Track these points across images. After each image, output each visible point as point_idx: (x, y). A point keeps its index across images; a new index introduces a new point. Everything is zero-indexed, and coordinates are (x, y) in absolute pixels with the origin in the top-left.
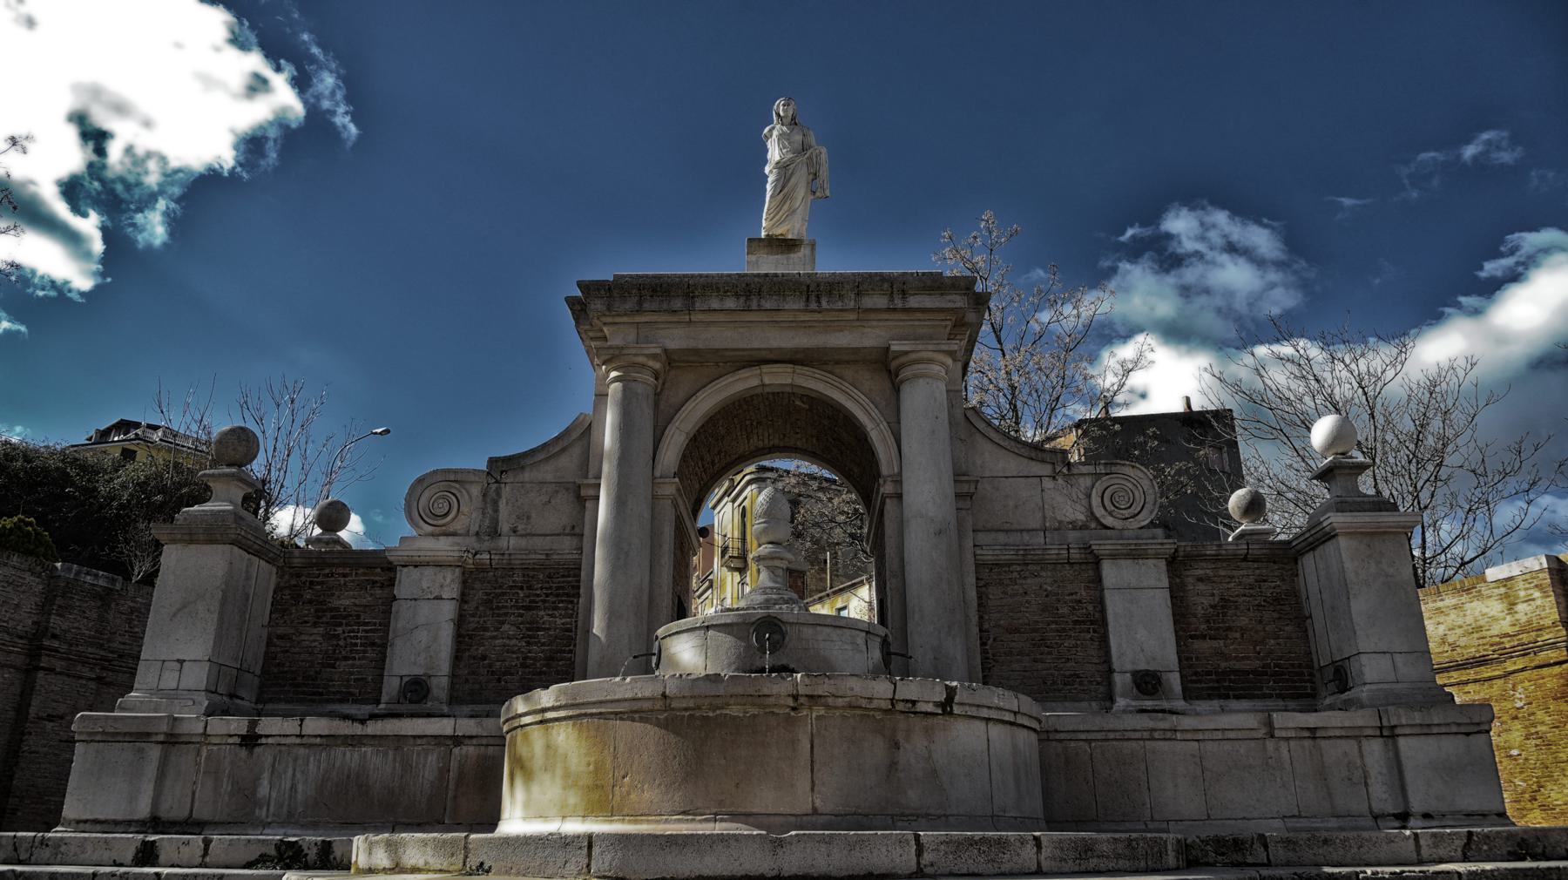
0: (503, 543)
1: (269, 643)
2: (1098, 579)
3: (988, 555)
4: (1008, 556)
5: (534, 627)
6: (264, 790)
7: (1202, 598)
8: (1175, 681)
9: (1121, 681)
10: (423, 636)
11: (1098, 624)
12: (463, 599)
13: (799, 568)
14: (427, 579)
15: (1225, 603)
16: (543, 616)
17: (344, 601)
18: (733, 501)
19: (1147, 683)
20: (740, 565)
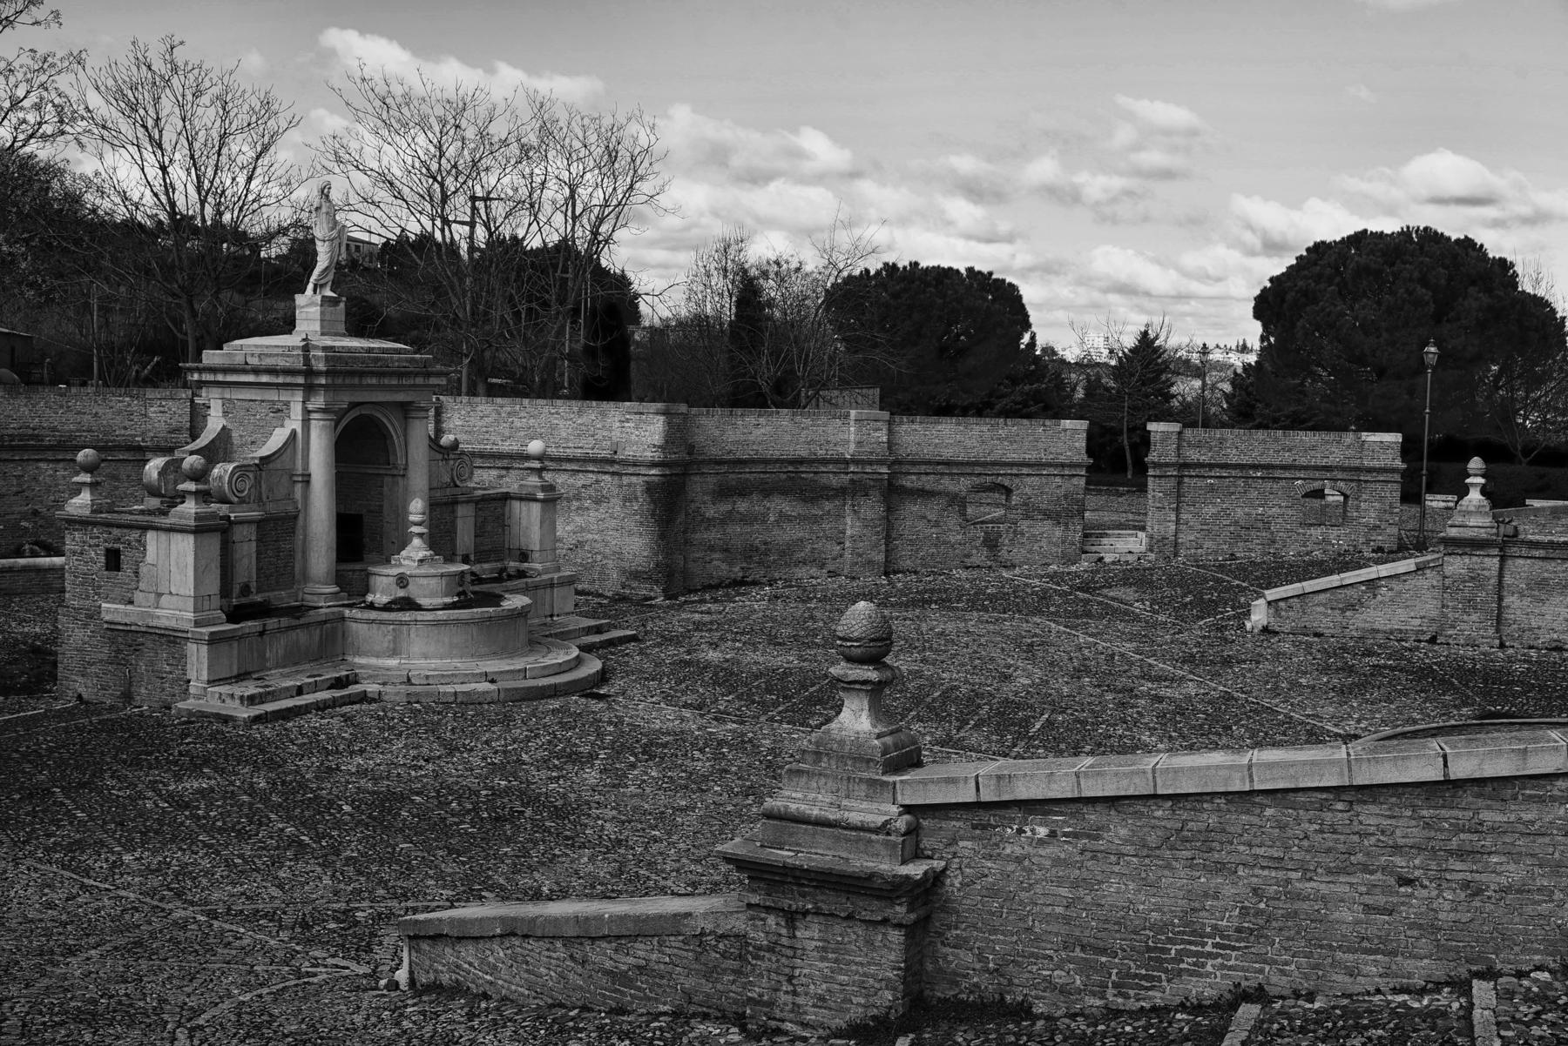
10: (246, 561)
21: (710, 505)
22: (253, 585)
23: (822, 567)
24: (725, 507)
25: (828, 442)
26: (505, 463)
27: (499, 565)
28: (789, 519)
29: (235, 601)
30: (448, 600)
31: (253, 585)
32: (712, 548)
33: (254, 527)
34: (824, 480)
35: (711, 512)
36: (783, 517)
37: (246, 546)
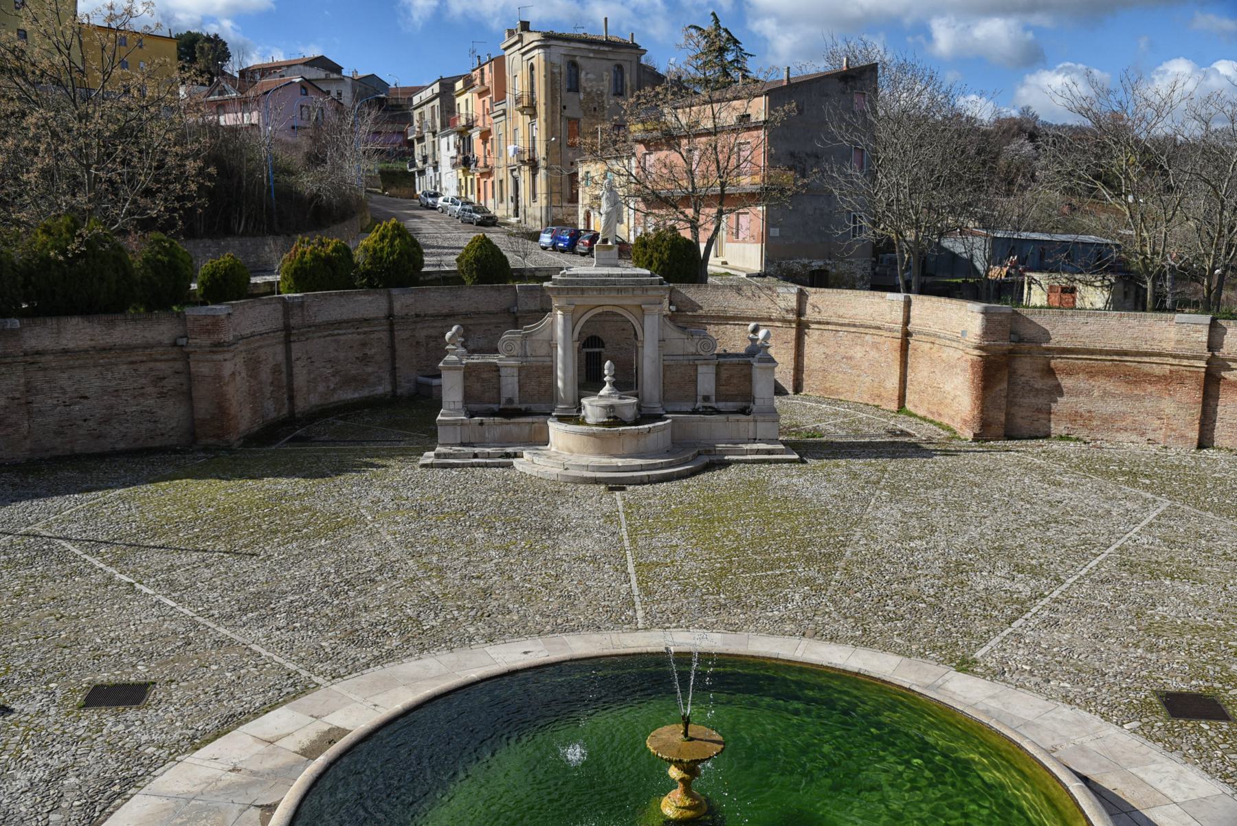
0: (529, 359)
2: (697, 370)
3: (666, 363)
4: (672, 363)
5: (540, 383)
6: (487, 435)
7: (724, 374)
9: (699, 398)
11: (695, 382)
12: (519, 375)
13: (575, 116)
14: (509, 371)
15: (731, 376)
18: (523, 54)
19: (706, 398)
22: (516, 399)
23: (1143, 434)
25: (1153, 339)
26: (932, 339)
27: (744, 404)
29: (501, 406)
30: (601, 420)
31: (516, 399)
34: (1146, 368)
36: (1105, 394)
37: (510, 379)
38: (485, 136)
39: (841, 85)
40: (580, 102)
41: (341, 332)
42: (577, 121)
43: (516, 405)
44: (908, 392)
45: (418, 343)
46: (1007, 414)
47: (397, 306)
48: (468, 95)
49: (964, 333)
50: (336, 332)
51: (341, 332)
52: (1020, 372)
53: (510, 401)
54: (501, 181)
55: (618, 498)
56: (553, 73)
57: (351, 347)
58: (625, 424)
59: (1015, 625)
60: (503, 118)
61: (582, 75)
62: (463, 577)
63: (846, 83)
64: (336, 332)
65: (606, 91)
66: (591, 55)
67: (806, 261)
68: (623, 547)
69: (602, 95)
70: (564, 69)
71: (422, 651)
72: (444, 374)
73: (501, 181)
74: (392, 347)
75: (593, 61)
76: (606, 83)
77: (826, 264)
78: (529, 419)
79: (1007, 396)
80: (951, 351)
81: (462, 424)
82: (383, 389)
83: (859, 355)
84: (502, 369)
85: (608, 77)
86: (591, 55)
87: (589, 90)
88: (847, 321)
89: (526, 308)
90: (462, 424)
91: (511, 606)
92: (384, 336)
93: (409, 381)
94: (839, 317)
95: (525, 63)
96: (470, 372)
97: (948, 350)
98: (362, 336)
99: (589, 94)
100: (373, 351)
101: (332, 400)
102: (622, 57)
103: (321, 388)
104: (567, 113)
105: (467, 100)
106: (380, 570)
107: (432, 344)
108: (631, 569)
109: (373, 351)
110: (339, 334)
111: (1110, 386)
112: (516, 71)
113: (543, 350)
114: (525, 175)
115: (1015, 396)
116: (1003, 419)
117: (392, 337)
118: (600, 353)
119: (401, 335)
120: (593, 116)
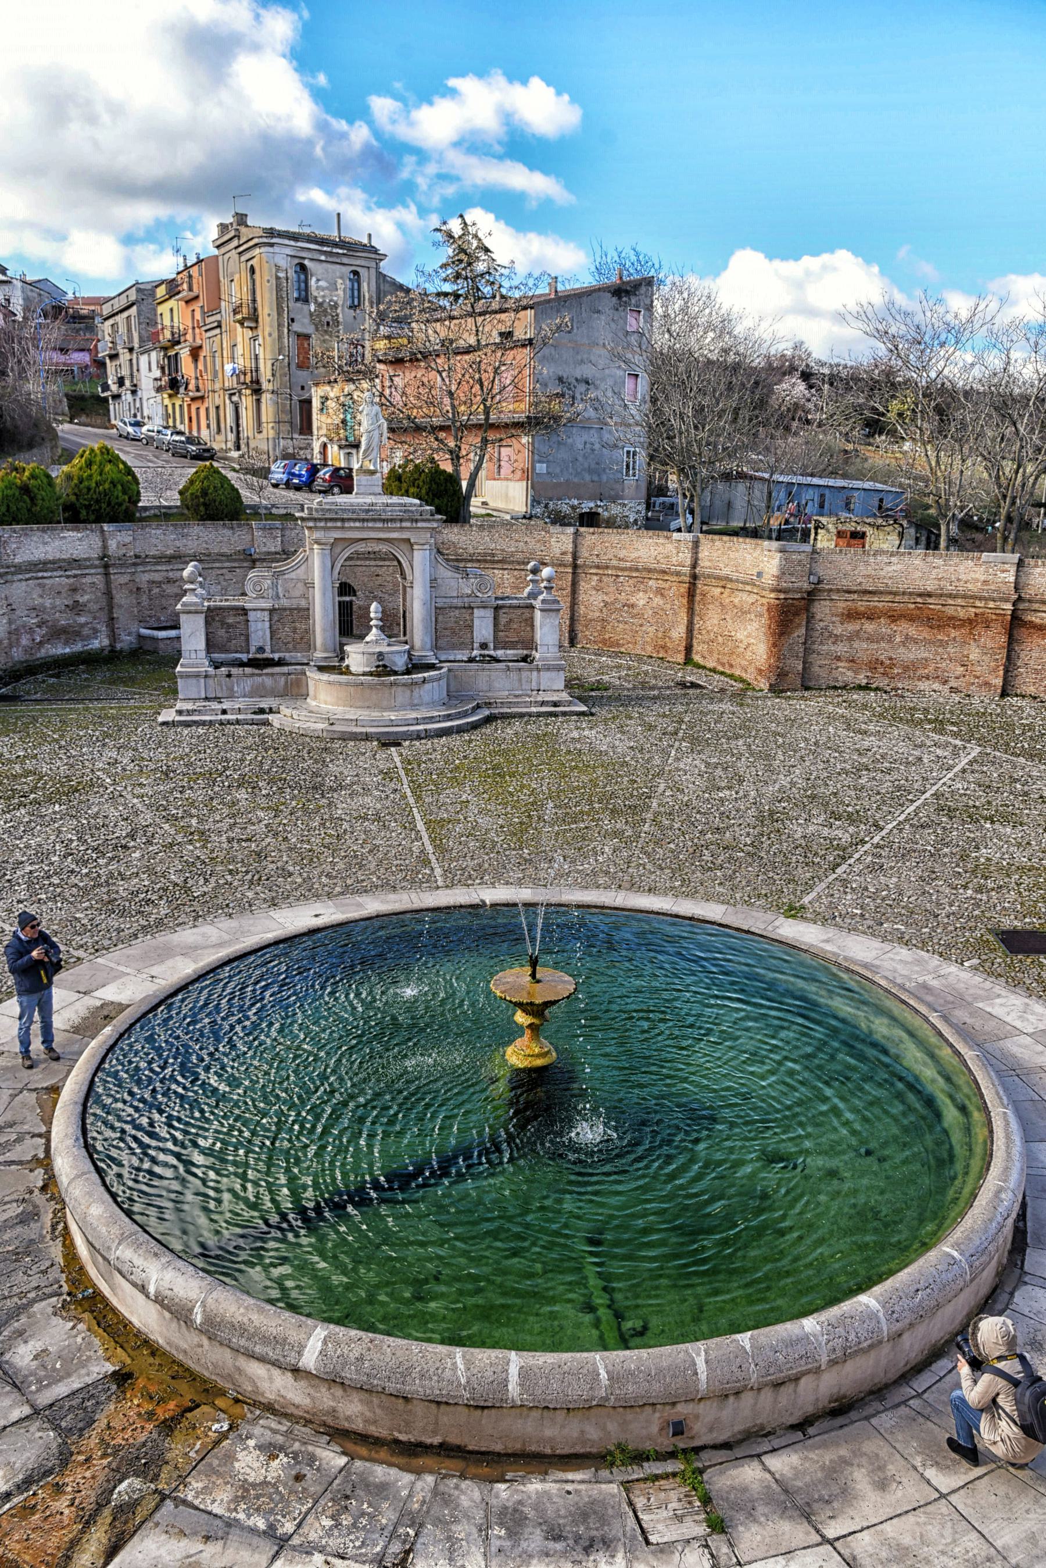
1: (207, 635)
8: (491, 645)
9: (476, 645)
10: (260, 633)
11: (471, 627)
16: (298, 625)
17: (230, 621)
19: (484, 646)
20: (253, 325)
21: (838, 625)
22: (268, 648)
23: (945, 682)
24: (852, 627)
25: (959, 580)
26: (722, 583)
27: (525, 652)
28: (916, 641)
30: (368, 669)
31: (268, 648)
32: (838, 659)
33: (267, 613)
34: (950, 611)
35: (838, 630)
37: (260, 625)
38: (195, 353)
39: (615, 299)
40: (311, 314)
41: (45, 574)
42: (307, 337)
43: (268, 655)
44: (695, 642)
45: (138, 589)
46: (804, 663)
47: (112, 544)
48: (172, 303)
49: (759, 574)
50: (40, 574)
51: (45, 574)
52: (818, 617)
53: (261, 650)
54: (218, 408)
55: (395, 754)
56: (278, 278)
57: (59, 593)
58: (396, 673)
59: (839, 871)
60: (217, 331)
61: (313, 282)
62: (230, 840)
63: (620, 298)
64: (40, 574)
65: (340, 303)
66: (323, 258)
67: (576, 502)
68: (408, 804)
69: (336, 306)
70: (291, 274)
71: (196, 919)
72: (183, 618)
73: (218, 408)
74: (109, 594)
75: (325, 265)
76: (341, 293)
77: (597, 506)
78: (285, 669)
79: (805, 643)
80: (744, 596)
81: (206, 676)
82: (99, 642)
83: (642, 603)
84: (250, 613)
85: (342, 286)
86: (323, 258)
87: (320, 300)
88: (628, 564)
89: (265, 549)
90: (206, 676)
91: (291, 869)
92: (99, 580)
93: (129, 634)
94: (620, 560)
95: (243, 265)
96: (212, 616)
97: (740, 594)
98: (72, 580)
99: (320, 305)
100: (86, 597)
101: (38, 655)
102: (358, 262)
103: (25, 641)
104: (296, 327)
105: (171, 310)
106: (132, 836)
107: (156, 591)
108: (420, 826)
109: (86, 597)
110: (43, 578)
111: (912, 630)
112: (232, 274)
113: (300, 589)
114: (247, 402)
115: (813, 643)
116: (800, 667)
117: (108, 583)
118: (351, 602)
119: (119, 579)
120: (326, 332)
